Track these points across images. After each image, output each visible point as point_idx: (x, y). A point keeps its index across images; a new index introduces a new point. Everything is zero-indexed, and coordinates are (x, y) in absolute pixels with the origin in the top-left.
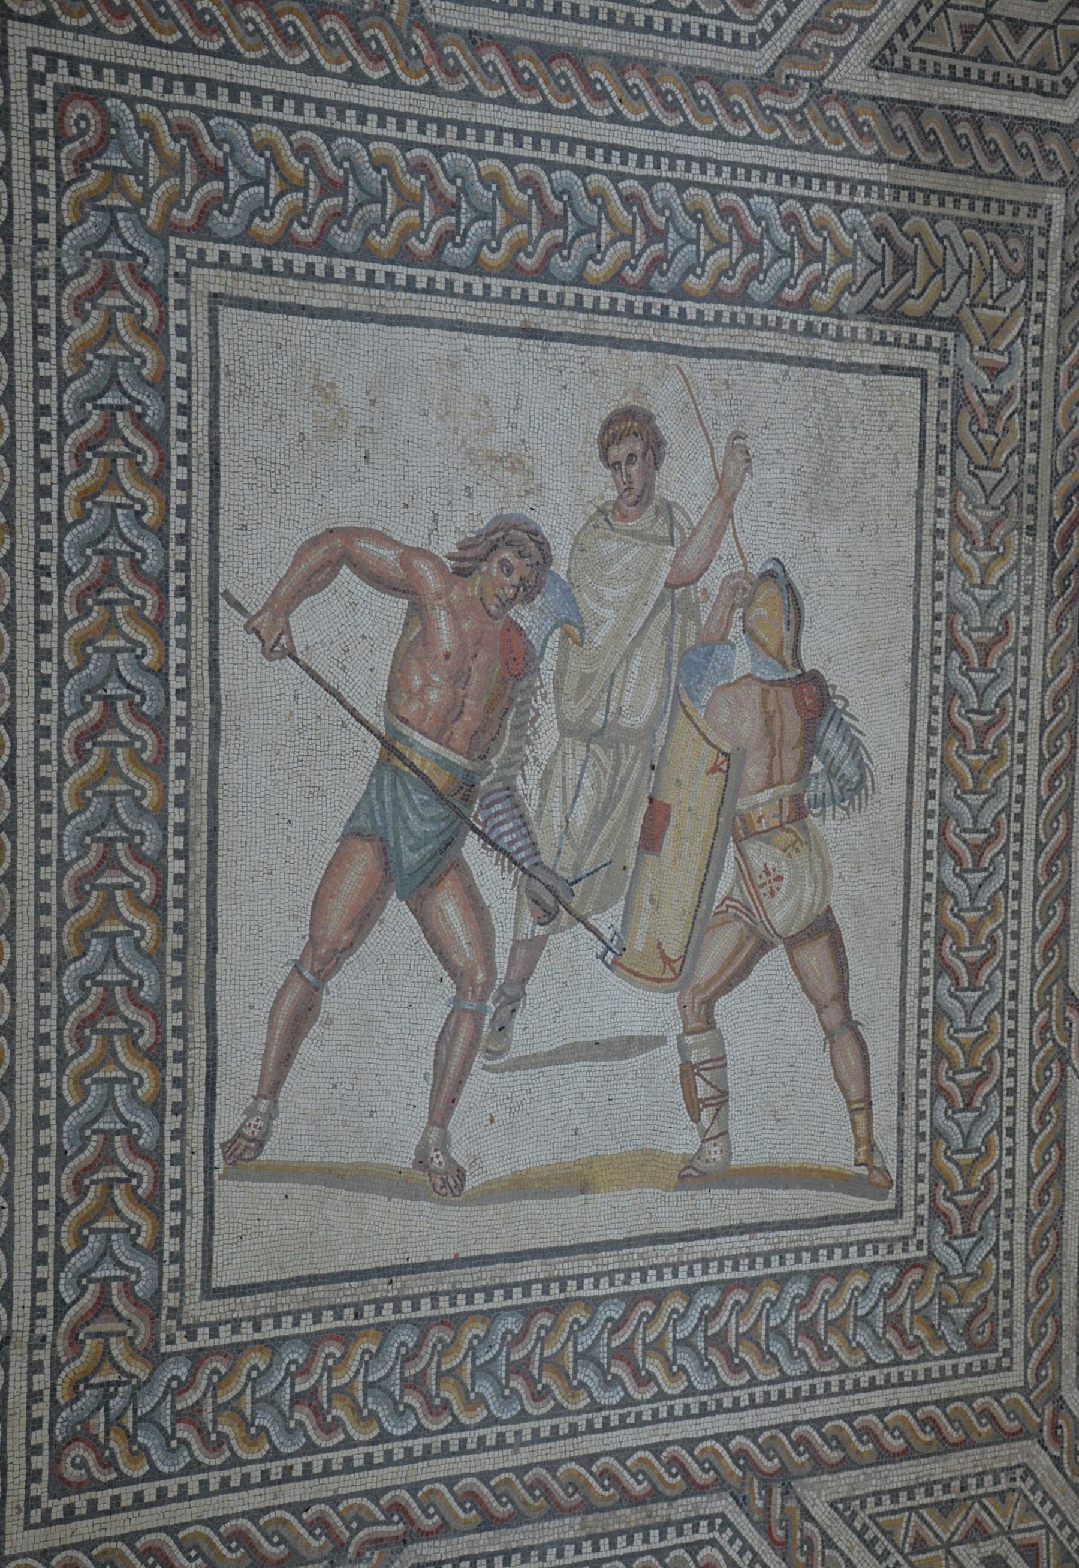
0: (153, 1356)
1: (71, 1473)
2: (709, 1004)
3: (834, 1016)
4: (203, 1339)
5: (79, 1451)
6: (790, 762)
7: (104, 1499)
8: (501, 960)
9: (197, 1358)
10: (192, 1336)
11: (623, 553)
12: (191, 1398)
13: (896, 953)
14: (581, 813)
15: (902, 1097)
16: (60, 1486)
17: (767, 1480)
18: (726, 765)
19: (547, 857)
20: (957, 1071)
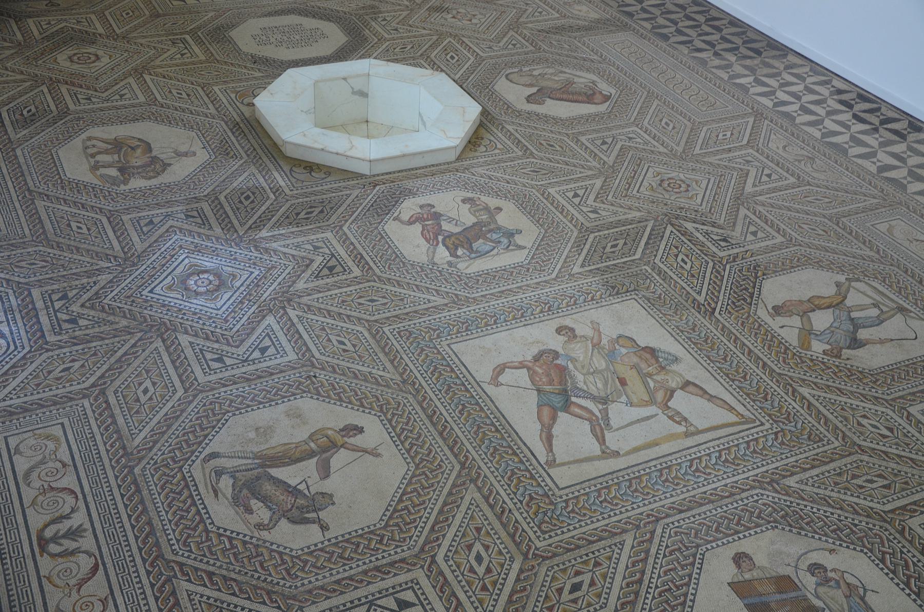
0: (551, 503)
2: (666, 404)
3: (708, 397)
5: (545, 525)
6: (653, 361)
7: (559, 532)
10: (561, 497)
14: (600, 385)
16: (544, 532)
17: (768, 483)
18: (634, 367)
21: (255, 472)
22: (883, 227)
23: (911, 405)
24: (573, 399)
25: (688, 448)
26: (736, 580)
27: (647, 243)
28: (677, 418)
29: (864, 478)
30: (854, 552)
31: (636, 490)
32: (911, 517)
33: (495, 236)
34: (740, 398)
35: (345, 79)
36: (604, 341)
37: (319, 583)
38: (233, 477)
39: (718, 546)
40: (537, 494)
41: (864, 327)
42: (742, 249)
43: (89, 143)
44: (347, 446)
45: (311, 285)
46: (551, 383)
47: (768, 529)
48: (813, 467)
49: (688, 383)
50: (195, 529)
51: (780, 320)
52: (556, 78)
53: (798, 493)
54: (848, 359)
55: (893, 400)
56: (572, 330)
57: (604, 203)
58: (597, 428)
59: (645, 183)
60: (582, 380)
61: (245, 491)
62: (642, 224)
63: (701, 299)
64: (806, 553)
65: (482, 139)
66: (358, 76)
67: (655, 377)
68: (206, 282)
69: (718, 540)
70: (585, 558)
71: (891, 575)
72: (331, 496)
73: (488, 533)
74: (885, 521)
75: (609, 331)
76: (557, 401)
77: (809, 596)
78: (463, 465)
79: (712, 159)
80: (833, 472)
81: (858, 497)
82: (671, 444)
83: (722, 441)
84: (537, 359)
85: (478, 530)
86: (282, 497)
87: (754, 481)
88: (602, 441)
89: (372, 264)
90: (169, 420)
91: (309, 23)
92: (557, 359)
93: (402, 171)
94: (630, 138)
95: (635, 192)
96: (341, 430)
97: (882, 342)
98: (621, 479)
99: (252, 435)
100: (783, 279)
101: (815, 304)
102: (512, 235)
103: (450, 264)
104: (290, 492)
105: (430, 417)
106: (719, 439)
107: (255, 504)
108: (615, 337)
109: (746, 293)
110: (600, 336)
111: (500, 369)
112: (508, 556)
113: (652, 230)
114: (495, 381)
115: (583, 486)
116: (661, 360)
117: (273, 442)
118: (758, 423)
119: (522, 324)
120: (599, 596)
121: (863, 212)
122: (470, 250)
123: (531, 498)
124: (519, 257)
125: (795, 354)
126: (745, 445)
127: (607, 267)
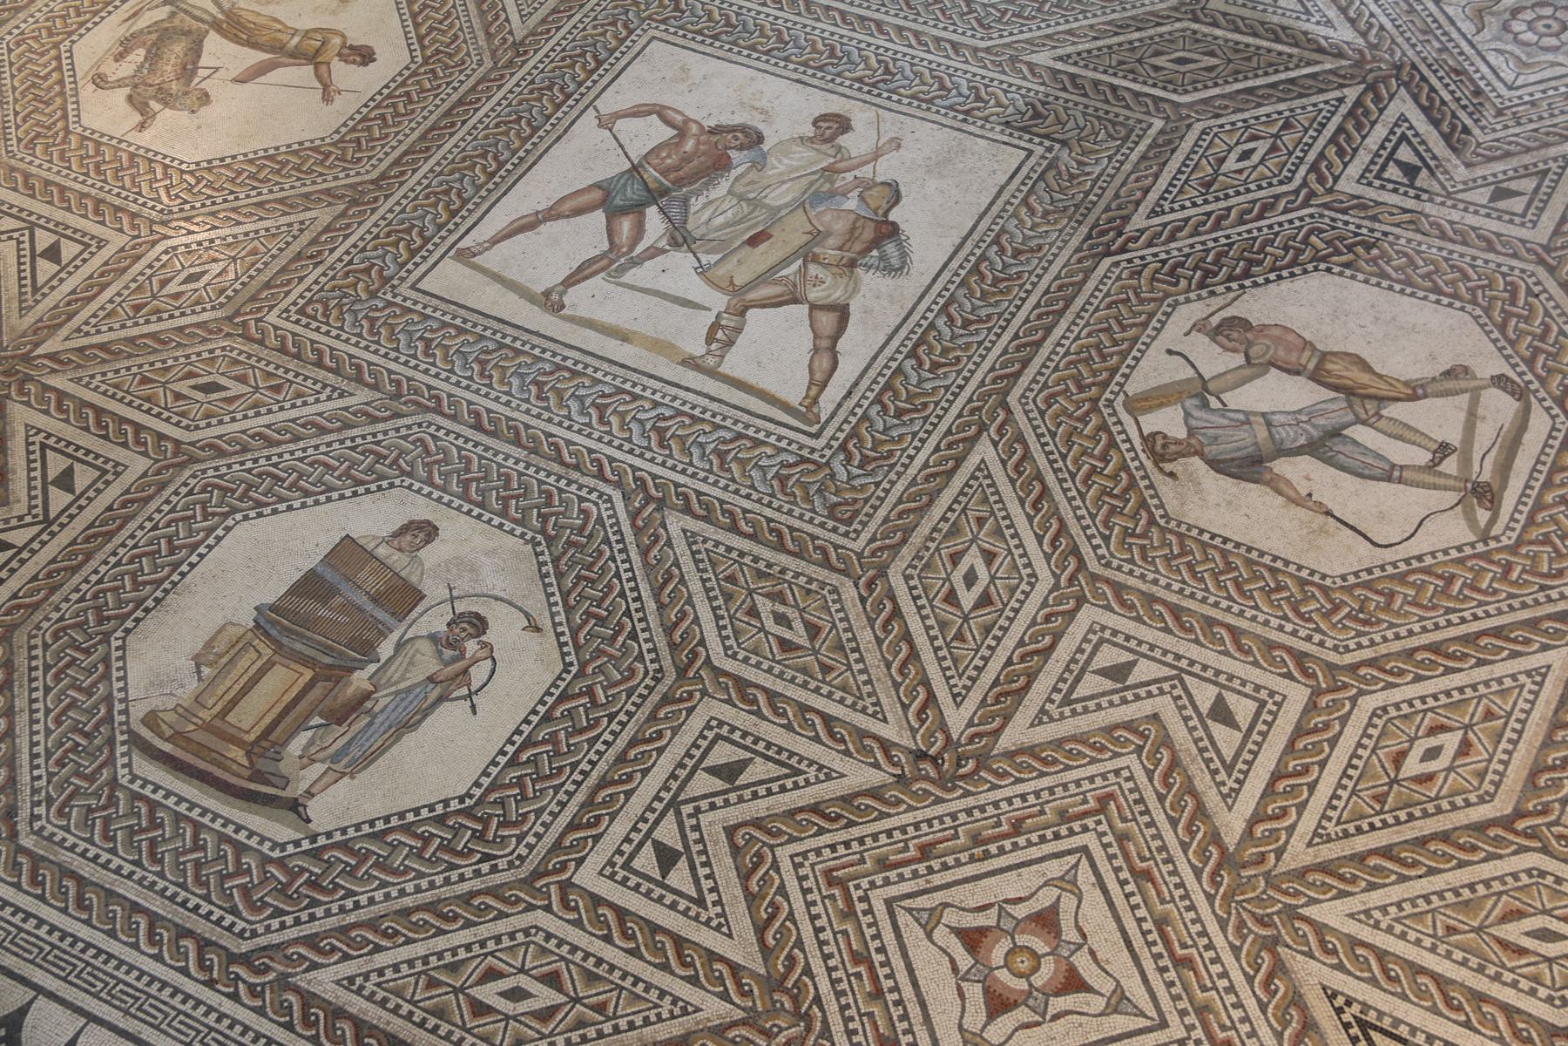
0: (373, 295)
1: (309, 310)
2: (747, 308)
4: (398, 300)
6: (858, 247)
7: (314, 325)
8: (639, 249)
9: (390, 304)
11: (804, 154)
13: (882, 339)
14: (720, 220)
15: (850, 393)
16: (302, 312)
17: (649, 499)
18: (817, 236)
21: (195, 24)
24: (652, 212)
25: (651, 376)
26: (362, 542)
28: (722, 335)
29: (781, 609)
30: (557, 655)
31: (483, 363)
32: (729, 701)
34: (865, 382)
36: (849, 176)
37: (34, 170)
38: (173, 14)
39: (429, 495)
41: (1330, 462)
44: (323, 68)
47: (522, 536)
48: (752, 537)
53: (656, 541)
54: (1172, 475)
55: (1095, 578)
61: (154, 36)
62: (1316, 56)
63: (1138, 221)
64: (497, 598)
69: (444, 490)
70: (280, 372)
71: (535, 719)
74: (682, 672)
77: (394, 637)
78: (383, 176)
80: (761, 565)
81: (718, 618)
82: (645, 353)
83: (715, 406)
84: (713, 131)
87: (636, 479)
88: (577, 276)
92: (741, 148)
96: (351, 47)
100: (1358, 294)
105: (460, 102)
106: (713, 399)
107: (139, 55)
116: (875, 253)
118: (814, 429)
119: (795, 76)
120: (208, 416)
123: (367, 271)
126: (728, 436)
127: (1096, 83)
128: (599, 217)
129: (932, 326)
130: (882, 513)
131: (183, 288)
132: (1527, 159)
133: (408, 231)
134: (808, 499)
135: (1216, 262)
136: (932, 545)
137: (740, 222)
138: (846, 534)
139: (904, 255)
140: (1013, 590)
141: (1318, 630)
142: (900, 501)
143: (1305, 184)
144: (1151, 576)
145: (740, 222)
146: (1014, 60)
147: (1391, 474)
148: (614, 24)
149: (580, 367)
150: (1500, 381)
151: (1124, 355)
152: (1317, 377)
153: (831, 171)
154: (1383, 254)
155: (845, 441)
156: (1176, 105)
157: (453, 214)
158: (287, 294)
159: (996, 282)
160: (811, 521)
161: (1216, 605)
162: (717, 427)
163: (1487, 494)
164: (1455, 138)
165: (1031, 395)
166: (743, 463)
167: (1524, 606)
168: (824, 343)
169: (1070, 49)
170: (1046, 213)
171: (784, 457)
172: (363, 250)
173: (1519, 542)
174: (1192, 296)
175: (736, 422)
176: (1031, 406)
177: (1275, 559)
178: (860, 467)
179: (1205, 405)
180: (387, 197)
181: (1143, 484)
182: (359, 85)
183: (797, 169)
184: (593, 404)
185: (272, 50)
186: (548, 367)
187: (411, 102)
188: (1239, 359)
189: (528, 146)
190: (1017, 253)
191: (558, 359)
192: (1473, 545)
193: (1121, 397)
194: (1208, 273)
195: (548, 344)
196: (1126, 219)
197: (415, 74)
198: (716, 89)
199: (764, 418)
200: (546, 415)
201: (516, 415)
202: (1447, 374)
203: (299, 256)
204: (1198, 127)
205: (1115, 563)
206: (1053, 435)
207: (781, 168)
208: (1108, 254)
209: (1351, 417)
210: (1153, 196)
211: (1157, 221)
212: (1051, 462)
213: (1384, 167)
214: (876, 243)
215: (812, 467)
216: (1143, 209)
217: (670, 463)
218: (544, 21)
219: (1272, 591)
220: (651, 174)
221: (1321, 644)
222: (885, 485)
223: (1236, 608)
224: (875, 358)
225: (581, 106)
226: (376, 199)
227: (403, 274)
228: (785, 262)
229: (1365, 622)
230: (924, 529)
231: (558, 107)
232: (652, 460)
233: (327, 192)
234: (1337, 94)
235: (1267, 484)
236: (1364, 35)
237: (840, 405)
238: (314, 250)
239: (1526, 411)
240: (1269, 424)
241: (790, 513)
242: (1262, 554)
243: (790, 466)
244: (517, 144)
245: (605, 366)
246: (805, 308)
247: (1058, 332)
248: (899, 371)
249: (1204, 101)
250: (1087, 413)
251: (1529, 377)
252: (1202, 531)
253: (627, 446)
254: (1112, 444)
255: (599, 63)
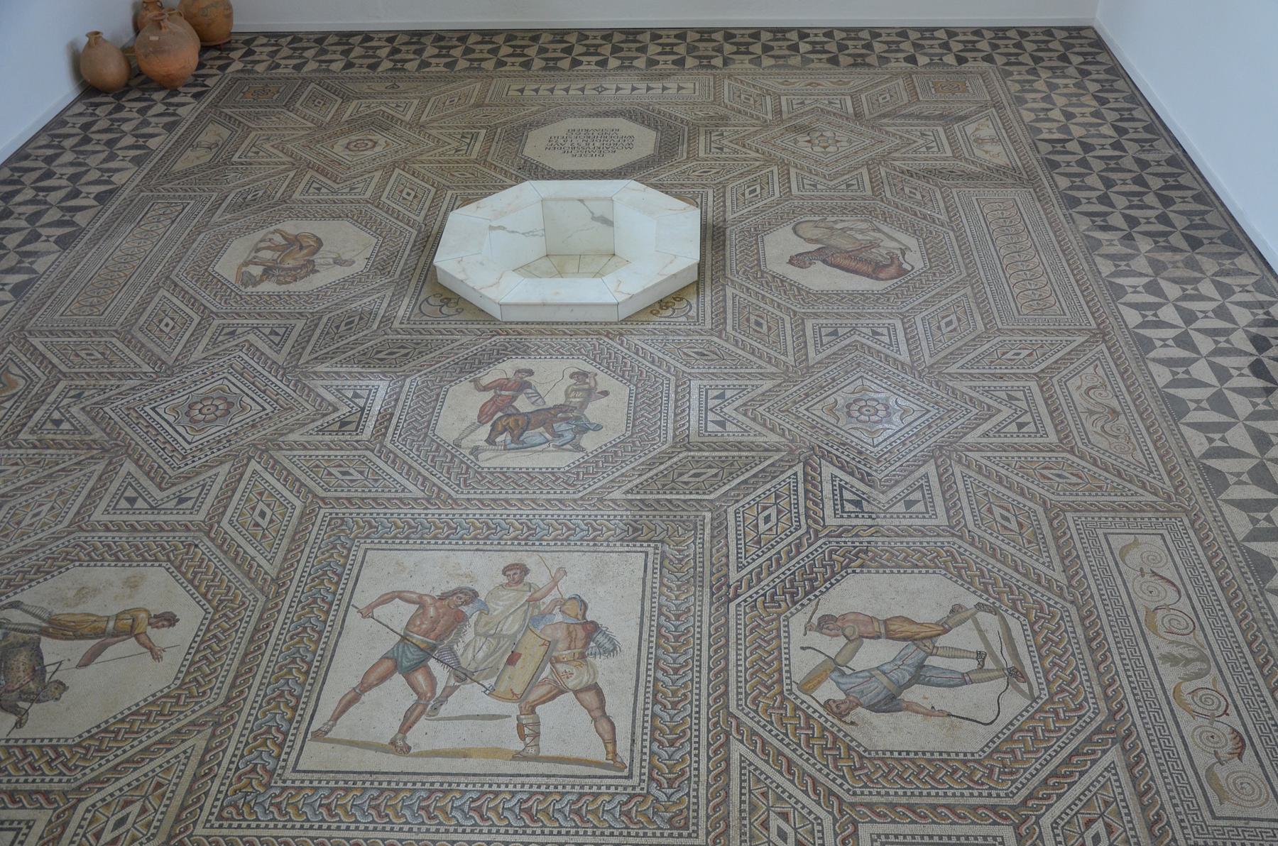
1: (225, 814)
4: (289, 783)
5: (231, 809)
6: (580, 644)
7: (235, 824)
8: (439, 691)
9: (284, 789)
10: (284, 781)
11: (509, 595)
12: (279, 800)
14: (480, 655)
18: (550, 645)
19: (464, 665)
20: (663, 730)
21: (27, 637)
22: (1117, 542)
23: (872, 821)
24: (432, 663)
25: (498, 775)
27: (745, 482)
28: (529, 730)
31: (376, 807)
33: (564, 426)
34: (639, 731)
35: (581, 201)
36: (548, 600)
40: (264, 766)
41: (928, 684)
42: (869, 522)
43: (270, 236)
44: (143, 638)
45: (303, 439)
46: (426, 634)
49: (596, 689)
50: (769, 688)
51: (816, 639)
52: (860, 237)
54: (852, 723)
55: (853, 805)
56: (525, 571)
57: (745, 415)
58: (420, 709)
59: (831, 400)
60: (467, 641)
62: (766, 454)
63: (734, 576)
65: (682, 299)
66: (598, 199)
67: (558, 666)
68: (205, 411)
72: (65, 688)
73: (163, 795)
75: (567, 588)
76: (412, 655)
78: (228, 699)
79: (962, 386)
83: (552, 780)
84: (442, 598)
85: (159, 785)
86: (22, 674)
88: (407, 724)
89: (391, 430)
90: (26, 551)
91: (624, 126)
92: (466, 603)
93: (543, 323)
94: (875, 333)
95: (802, 409)
96: (155, 616)
97: (931, 713)
98: (376, 784)
99: (71, 594)
100: (880, 580)
101: (888, 630)
102: (586, 430)
103: (475, 451)
104: (34, 670)
105: (256, 630)
106: (548, 776)
108: (567, 597)
109: (806, 586)
110: (551, 589)
111: (386, 599)
112: (152, 831)
113: (773, 465)
114: (367, 613)
115: (324, 777)
116: (592, 644)
117: (80, 609)
118: (626, 773)
121: (1114, 510)
122: (516, 439)
123: (254, 770)
124: (562, 460)
125: (781, 693)
126: (574, 798)
127: (658, 501)
128: (398, 679)
129: (656, 679)
130: (702, 813)
131: (117, 833)
132: (909, 481)
133: (268, 731)
134: (651, 821)
135: (792, 586)
136: (746, 822)
137: (494, 652)
138: (689, 836)
139: (611, 640)
140: (812, 832)
141: (991, 788)
142: (708, 802)
143: (809, 527)
144: (883, 792)
145: (494, 652)
146: (601, 500)
147: (965, 680)
148: (334, 547)
149: (446, 786)
150: (979, 606)
151: (779, 659)
152: (890, 636)
153: (533, 601)
154: (876, 555)
155: (650, 774)
156: (711, 501)
157: (295, 709)
158: (201, 808)
159: (677, 639)
160: (662, 836)
161: (929, 795)
162: (563, 794)
163: (1016, 674)
164: (866, 478)
165: (743, 702)
166: (594, 812)
167: (1078, 732)
168: (597, 714)
169: (630, 485)
170: (679, 587)
171: (618, 798)
172: (242, 756)
173: (1051, 696)
174: (793, 610)
175: (573, 787)
176: (747, 710)
177: (941, 753)
178: (670, 787)
179: (843, 674)
180: (239, 712)
181: (841, 735)
182: (176, 640)
183: (511, 606)
184: (470, 809)
185: (96, 636)
186: (424, 794)
187: (220, 641)
188: (843, 641)
189: (322, 646)
190: (678, 617)
191: (427, 786)
192: (1030, 705)
193: (794, 686)
194: (792, 595)
195: (415, 778)
196: (726, 576)
197: (212, 621)
198: (433, 570)
199: (586, 777)
200: (442, 829)
201: (421, 836)
202: (952, 611)
203: (195, 778)
204: (731, 510)
205: (858, 791)
206: (771, 723)
207: (500, 609)
208: (730, 601)
209: (923, 654)
210: (733, 558)
211: (744, 572)
212: (782, 741)
213: (842, 505)
214: (589, 638)
215: (641, 799)
216: (733, 567)
217: (547, 831)
218: (285, 559)
219: (952, 774)
220: (417, 638)
221: (998, 796)
222: (693, 793)
223: (941, 793)
224: (634, 712)
225: (343, 608)
226: (232, 717)
227: (282, 764)
228: (539, 669)
229: (1011, 773)
230: (735, 814)
231: (328, 613)
232: (534, 833)
233: (193, 723)
234: (790, 472)
235: (907, 709)
236: (783, 435)
237: (632, 751)
238: (205, 769)
239: (1003, 618)
240: (884, 673)
241: (645, 835)
242: (932, 754)
243: (626, 803)
244: (313, 647)
245: (463, 779)
246: (571, 695)
247: (732, 657)
248: (654, 715)
249: (725, 494)
250: (782, 702)
251: (992, 600)
252: (892, 752)
253: (511, 831)
254: (808, 717)
255: (340, 576)
